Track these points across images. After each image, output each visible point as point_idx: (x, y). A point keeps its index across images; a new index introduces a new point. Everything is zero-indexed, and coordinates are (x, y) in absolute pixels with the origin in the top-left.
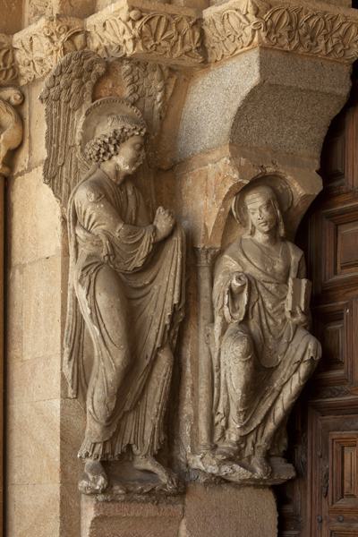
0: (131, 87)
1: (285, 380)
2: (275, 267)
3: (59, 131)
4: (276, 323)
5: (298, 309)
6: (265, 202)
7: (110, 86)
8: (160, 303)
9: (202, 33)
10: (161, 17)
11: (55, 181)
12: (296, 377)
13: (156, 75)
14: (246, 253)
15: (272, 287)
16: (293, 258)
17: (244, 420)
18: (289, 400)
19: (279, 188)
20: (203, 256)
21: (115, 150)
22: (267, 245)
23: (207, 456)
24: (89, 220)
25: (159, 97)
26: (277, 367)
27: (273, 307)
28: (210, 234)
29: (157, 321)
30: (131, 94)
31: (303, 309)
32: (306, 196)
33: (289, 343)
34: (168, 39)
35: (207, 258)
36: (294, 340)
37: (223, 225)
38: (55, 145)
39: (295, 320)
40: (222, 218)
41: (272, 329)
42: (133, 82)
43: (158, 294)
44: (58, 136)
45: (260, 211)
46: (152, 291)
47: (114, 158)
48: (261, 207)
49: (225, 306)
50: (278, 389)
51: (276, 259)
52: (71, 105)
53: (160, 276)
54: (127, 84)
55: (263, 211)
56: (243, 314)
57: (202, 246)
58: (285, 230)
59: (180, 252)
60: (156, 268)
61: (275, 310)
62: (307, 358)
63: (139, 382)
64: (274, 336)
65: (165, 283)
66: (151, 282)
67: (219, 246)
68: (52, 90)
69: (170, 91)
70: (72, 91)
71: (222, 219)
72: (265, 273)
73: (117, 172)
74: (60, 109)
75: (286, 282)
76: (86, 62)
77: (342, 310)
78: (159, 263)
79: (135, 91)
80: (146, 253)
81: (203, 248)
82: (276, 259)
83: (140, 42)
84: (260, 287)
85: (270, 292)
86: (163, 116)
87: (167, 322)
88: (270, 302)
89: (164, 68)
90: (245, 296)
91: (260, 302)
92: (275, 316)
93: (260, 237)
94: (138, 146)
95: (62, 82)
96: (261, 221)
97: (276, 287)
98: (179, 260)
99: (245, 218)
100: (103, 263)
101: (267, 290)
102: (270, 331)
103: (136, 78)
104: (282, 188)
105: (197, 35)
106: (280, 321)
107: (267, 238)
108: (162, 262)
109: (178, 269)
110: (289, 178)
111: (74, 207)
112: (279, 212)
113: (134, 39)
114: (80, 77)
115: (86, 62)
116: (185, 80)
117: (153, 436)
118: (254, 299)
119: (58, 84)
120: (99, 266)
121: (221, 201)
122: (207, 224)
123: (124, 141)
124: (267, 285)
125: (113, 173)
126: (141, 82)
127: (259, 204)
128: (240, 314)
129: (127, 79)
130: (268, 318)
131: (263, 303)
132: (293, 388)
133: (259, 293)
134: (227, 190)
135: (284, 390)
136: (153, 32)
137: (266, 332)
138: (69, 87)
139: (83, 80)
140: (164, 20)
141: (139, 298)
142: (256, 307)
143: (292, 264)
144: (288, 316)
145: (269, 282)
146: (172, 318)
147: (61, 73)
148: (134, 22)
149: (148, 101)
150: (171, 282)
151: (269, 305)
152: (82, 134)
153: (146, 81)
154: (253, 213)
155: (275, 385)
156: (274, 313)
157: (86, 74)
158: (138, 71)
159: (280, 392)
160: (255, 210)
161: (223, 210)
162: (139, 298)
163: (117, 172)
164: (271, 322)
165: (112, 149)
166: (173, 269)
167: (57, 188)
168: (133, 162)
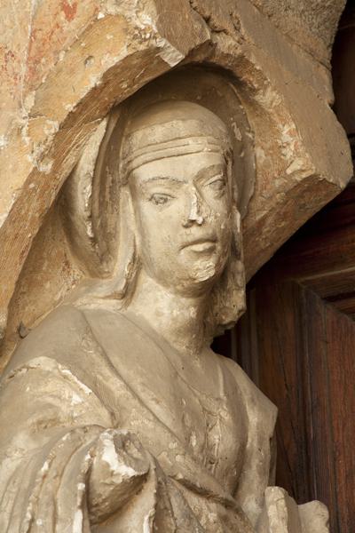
6: (217, 160)
40: (35, 204)
48: (200, 176)
55: (210, 193)
71: (34, 209)
96: (196, 232)
154: (163, 200)
160: (177, 183)
161: (47, 167)
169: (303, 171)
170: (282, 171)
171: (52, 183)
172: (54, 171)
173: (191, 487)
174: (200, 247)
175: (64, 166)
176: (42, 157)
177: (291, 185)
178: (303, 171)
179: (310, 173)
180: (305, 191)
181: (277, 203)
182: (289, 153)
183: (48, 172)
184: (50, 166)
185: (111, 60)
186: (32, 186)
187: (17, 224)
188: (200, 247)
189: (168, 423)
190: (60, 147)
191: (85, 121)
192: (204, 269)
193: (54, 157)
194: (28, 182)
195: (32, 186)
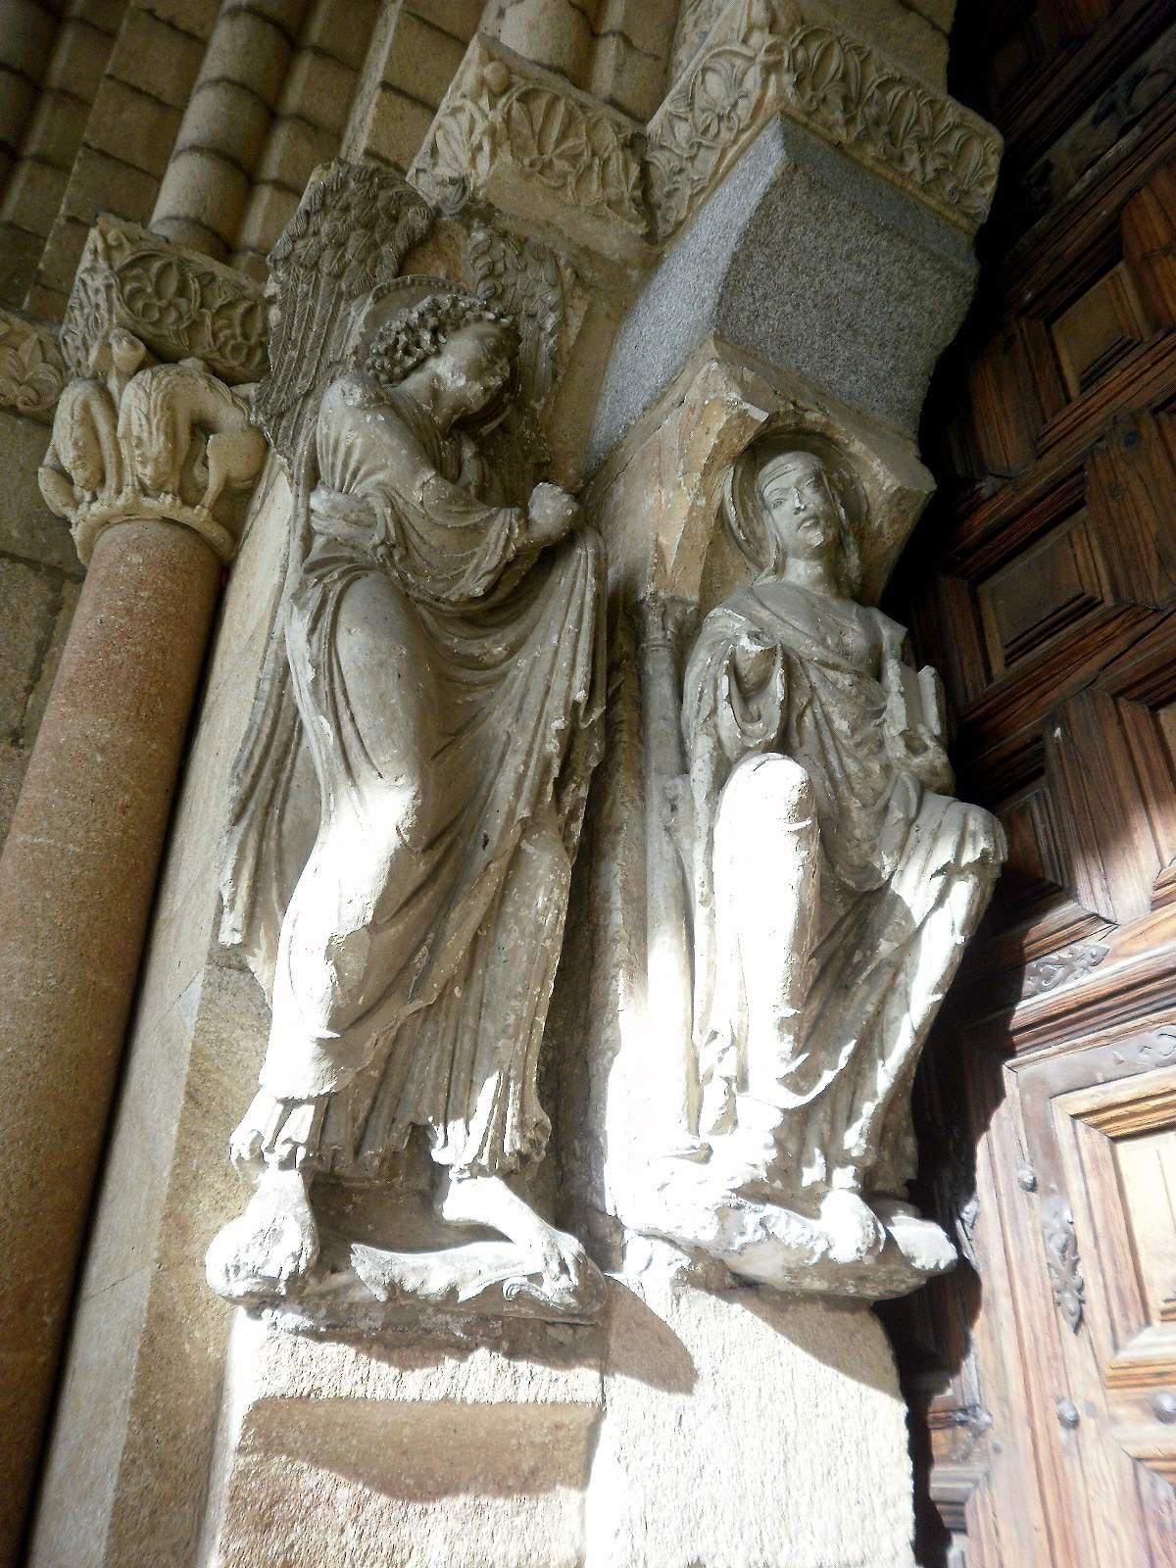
0: (489, 283)
3: (309, 328)
5: (922, 729)
8: (533, 700)
9: (645, 167)
10: (556, 99)
11: (284, 423)
13: (546, 273)
20: (653, 619)
21: (435, 341)
22: (819, 591)
24: (345, 465)
25: (550, 323)
27: (854, 729)
29: (521, 742)
31: (937, 731)
32: (901, 496)
34: (573, 158)
35: (664, 629)
36: (924, 815)
38: (295, 354)
39: (917, 761)
42: (491, 273)
43: (528, 677)
44: (305, 338)
45: (800, 492)
47: (432, 363)
49: (723, 705)
53: (539, 633)
54: (480, 273)
56: (777, 723)
57: (650, 589)
58: (860, 557)
61: (858, 738)
65: (549, 649)
66: (513, 650)
67: (695, 598)
68: (300, 244)
70: (348, 256)
71: (700, 528)
74: (316, 286)
75: (878, 674)
76: (383, 195)
77: (1038, 739)
78: (534, 610)
80: (495, 561)
81: (654, 595)
83: (506, 146)
87: (553, 747)
88: (844, 717)
89: (562, 263)
90: (777, 686)
93: (802, 572)
95: (325, 228)
98: (589, 597)
99: (759, 530)
100: (370, 568)
102: (852, 789)
103: (500, 266)
105: (635, 170)
106: (876, 767)
107: (820, 569)
108: (545, 605)
109: (587, 617)
111: (313, 444)
113: (492, 132)
119: (316, 233)
120: (355, 571)
122: (662, 540)
123: (457, 328)
124: (831, 674)
125: (425, 394)
126: (511, 280)
127: (793, 477)
128: (767, 725)
129: (480, 263)
130: (843, 754)
136: (537, 129)
137: (843, 789)
138: (341, 245)
139: (377, 236)
140: (561, 108)
142: (808, 720)
143: (886, 646)
144: (897, 750)
146: (570, 739)
147: (323, 204)
148: (494, 97)
150: (566, 645)
151: (842, 725)
152: (361, 334)
156: (858, 745)
157: (383, 221)
163: (435, 395)
165: (427, 337)
166: (572, 616)
167: (286, 436)
168: (476, 371)
170: (880, 490)
172: (708, 504)
173: (826, 665)
174: (808, 524)
176: (697, 497)
182: (881, 477)
185: (719, 426)
188: (808, 524)
189: (806, 630)
190: (705, 491)
191: (719, 469)
192: (816, 538)
194: (690, 513)
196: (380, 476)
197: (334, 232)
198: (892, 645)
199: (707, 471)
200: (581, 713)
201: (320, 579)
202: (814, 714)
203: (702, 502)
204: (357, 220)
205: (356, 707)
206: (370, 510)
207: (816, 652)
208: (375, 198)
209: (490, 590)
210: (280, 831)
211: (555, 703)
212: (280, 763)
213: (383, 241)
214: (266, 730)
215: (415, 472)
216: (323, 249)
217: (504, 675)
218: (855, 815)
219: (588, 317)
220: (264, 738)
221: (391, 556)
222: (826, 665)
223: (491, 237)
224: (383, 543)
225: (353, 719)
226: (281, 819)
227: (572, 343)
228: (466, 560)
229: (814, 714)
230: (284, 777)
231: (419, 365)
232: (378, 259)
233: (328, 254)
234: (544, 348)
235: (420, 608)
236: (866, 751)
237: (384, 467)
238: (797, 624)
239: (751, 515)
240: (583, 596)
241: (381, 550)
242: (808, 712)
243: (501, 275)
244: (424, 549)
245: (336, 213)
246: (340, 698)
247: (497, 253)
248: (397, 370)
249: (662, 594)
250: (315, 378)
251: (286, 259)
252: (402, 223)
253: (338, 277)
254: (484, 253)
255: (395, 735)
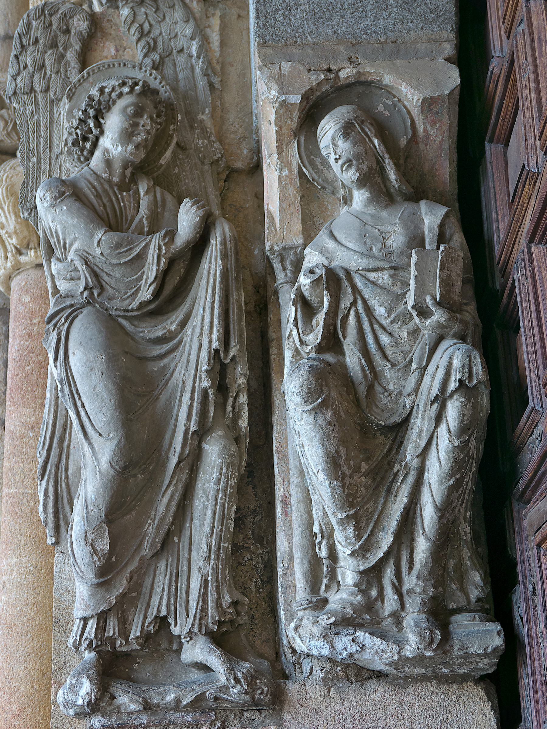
0: (143, 42)
1: (423, 443)
2: (390, 242)
4: (397, 341)
7: (113, 52)
12: (442, 430)
14: (336, 233)
15: (384, 278)
16: (426, 221)
17: (358, 537)
18: (441, 483)
19: (381, 108)
22: (371, 210)
23: (305, 622)
26: (406, 420)
27: (389, 312)
28: (278, 225)
30: (146, 56)
33: (423, 370)
37: (296, 200)
38: (34, 159)
41: (389, 352)
42: (142, 34)
46: (185, 339)
50: (415, 463)
51: (389, 228)
52: (51, 94)
54: (134, 39)
59: (219, 262)
60: (189, 301)
62: (453, 385)
63: (166, 499)
64: (393, 365)
66: (183, 324)
68: (19, 79)
69: (215, 38)
70: (48, 73)
72: (369, 255)
73: (108, 163)
76: (55, 20)
79: (151, 49)
81: (271, 249)
82: (389, 228)
84: (359, 282)
85: (382, 288)
86: (216, 80)
88: (382, 305)
91: (360, 306)
92: (394, 328)
94: (131, 110)
95: (29, 62)
97: (392, 276)
99: (330, 177)
101: (374, 283)
102: (385, 356)
103: (146, 26)
104: (386, 107)
107: (367, 194)
110: (388, 79)
112: (376, 141)
114: (54, 45)
115: (55, 20)
116: (239, 16)
117: (203, 597)
118: (345, 303)
119: (25, 67)
121: (275, 156)
124: (372, 276)
126: (157, 32)
129: (132, 31)
131: (369, 310)
132: (442, 454)
133: (355, 289)
134: (274, 128)
135: (428, 463)
141: (161, 357)
145: (375, 270)
147: (22, 46)
149: (181, 60)
151: (380, 311)
153: (164, 28)
155: (408, 458)
156: (392, 322)
157: (62, 39)
158: (146, 14)
159: (421, 471)
162: (161, 357)
164: (385, 339)
169: (419, 99)
171: (293, 177)
172: (290, 172)
175: (293, 167)
177: (420, 108)
178: (419, 99)
179: (422, 98)
180: (429, 107)
181: (423, 119)
183: (288, 174)
184: (287, 171)
186: (283, 183)
187: (287, 201)
193: (286, 167)
195: (283, 183)
196: (76, 246)
197: (34, 61)
198: (430, 230)
199: (280, 150)
200: (222, 355)
201: (55, 326)
202: (357, 313)
203: (286, 172)
204: (45, 46)
205: (84, 399)
206: (76, 270)
207: (362, 263)
208: (51, 24)
209: (157, 294)
210: (67, 477)
211: (204, 354)
212: (62, 440)
213: (65, 49)
214: (51, 422)
215: (92, 236)
216: (32, 76)
217: (180, 342)
218: (388, 374)
219: (224, 27)
220: (50, 427)
221: (92, 294)
222: (369, 270)
223: (132, 8)
224: (85, 289)
225: (83, 406)
226: (67, 470)
227: (218, 54)
228: (140, 279)
229: (357, 313)
230: (65, 445)
231: (95, 145)
232: (67, 63)
233: (36, 77)
234: (198, 70)
235: (120, 320)
236: (399, 324)
237: (75, 239)
238: (350, 245)
239: (321, 167)
240: (215, 274)
241: (86, 294)
242: (352, 313)
243: (149, 32)
244: (112, 282)
245: (31, 48)
246: (76, 396)
247: (141, 18)
248: (85, 153)
249: (276, 248)
250: (50, 171)
251: (15, 93)
252: (73, 31)
253: (47, 90)
254: (133, 22)
255: (104, 410)
